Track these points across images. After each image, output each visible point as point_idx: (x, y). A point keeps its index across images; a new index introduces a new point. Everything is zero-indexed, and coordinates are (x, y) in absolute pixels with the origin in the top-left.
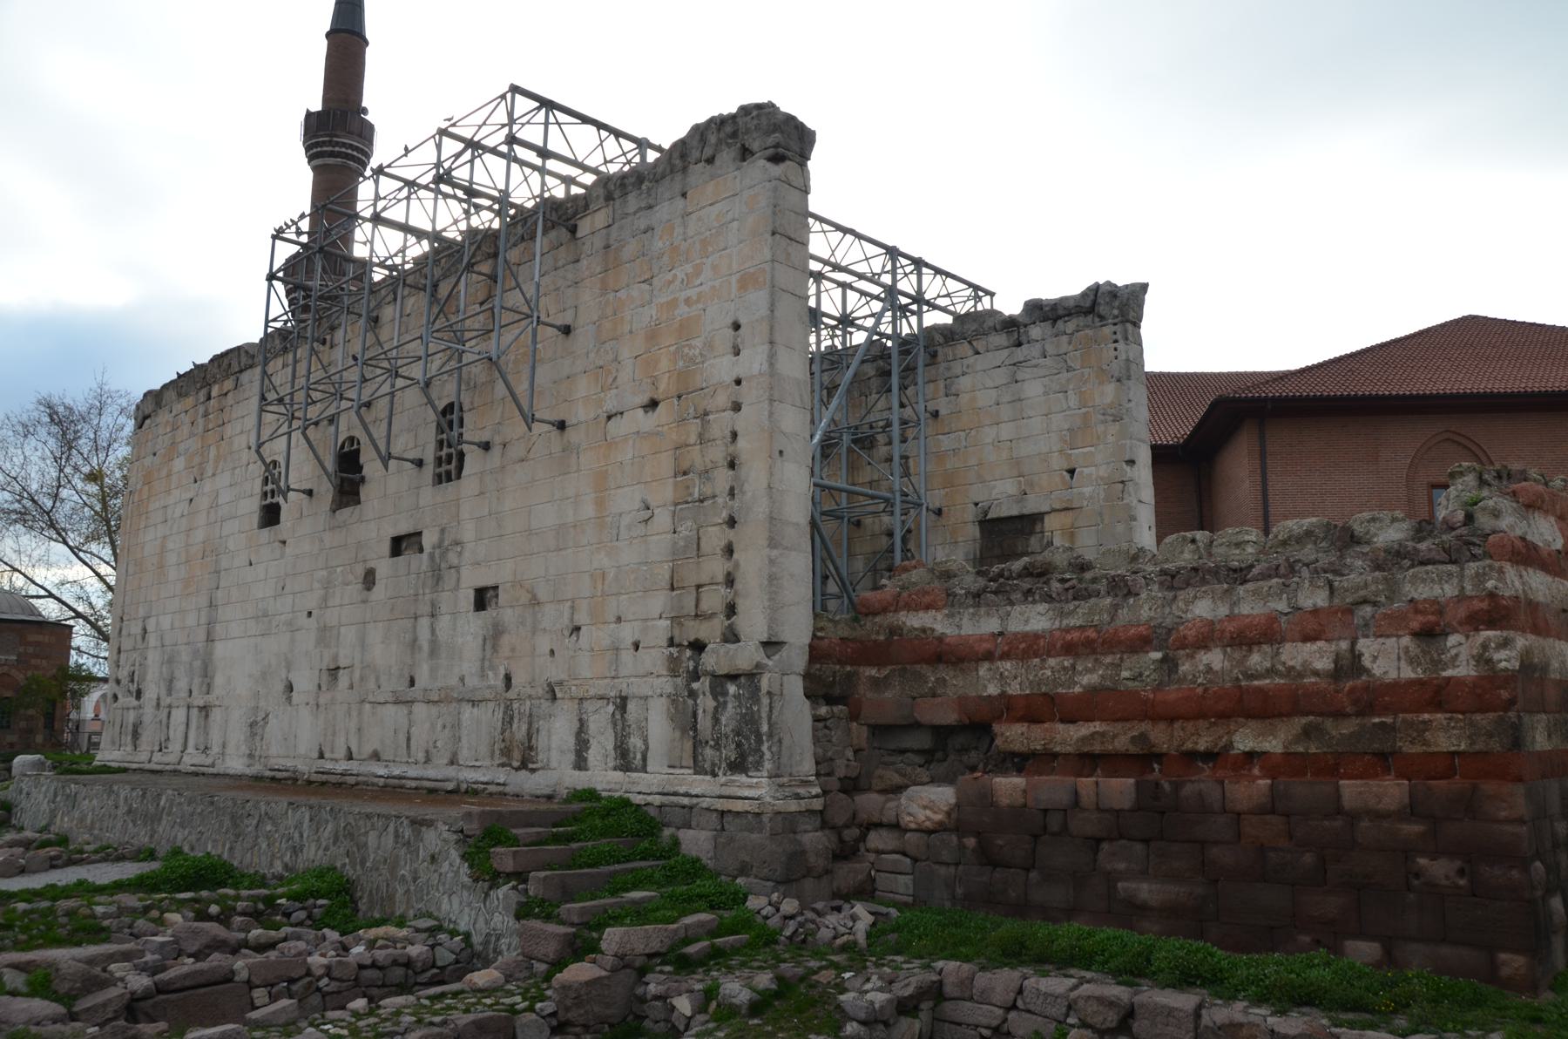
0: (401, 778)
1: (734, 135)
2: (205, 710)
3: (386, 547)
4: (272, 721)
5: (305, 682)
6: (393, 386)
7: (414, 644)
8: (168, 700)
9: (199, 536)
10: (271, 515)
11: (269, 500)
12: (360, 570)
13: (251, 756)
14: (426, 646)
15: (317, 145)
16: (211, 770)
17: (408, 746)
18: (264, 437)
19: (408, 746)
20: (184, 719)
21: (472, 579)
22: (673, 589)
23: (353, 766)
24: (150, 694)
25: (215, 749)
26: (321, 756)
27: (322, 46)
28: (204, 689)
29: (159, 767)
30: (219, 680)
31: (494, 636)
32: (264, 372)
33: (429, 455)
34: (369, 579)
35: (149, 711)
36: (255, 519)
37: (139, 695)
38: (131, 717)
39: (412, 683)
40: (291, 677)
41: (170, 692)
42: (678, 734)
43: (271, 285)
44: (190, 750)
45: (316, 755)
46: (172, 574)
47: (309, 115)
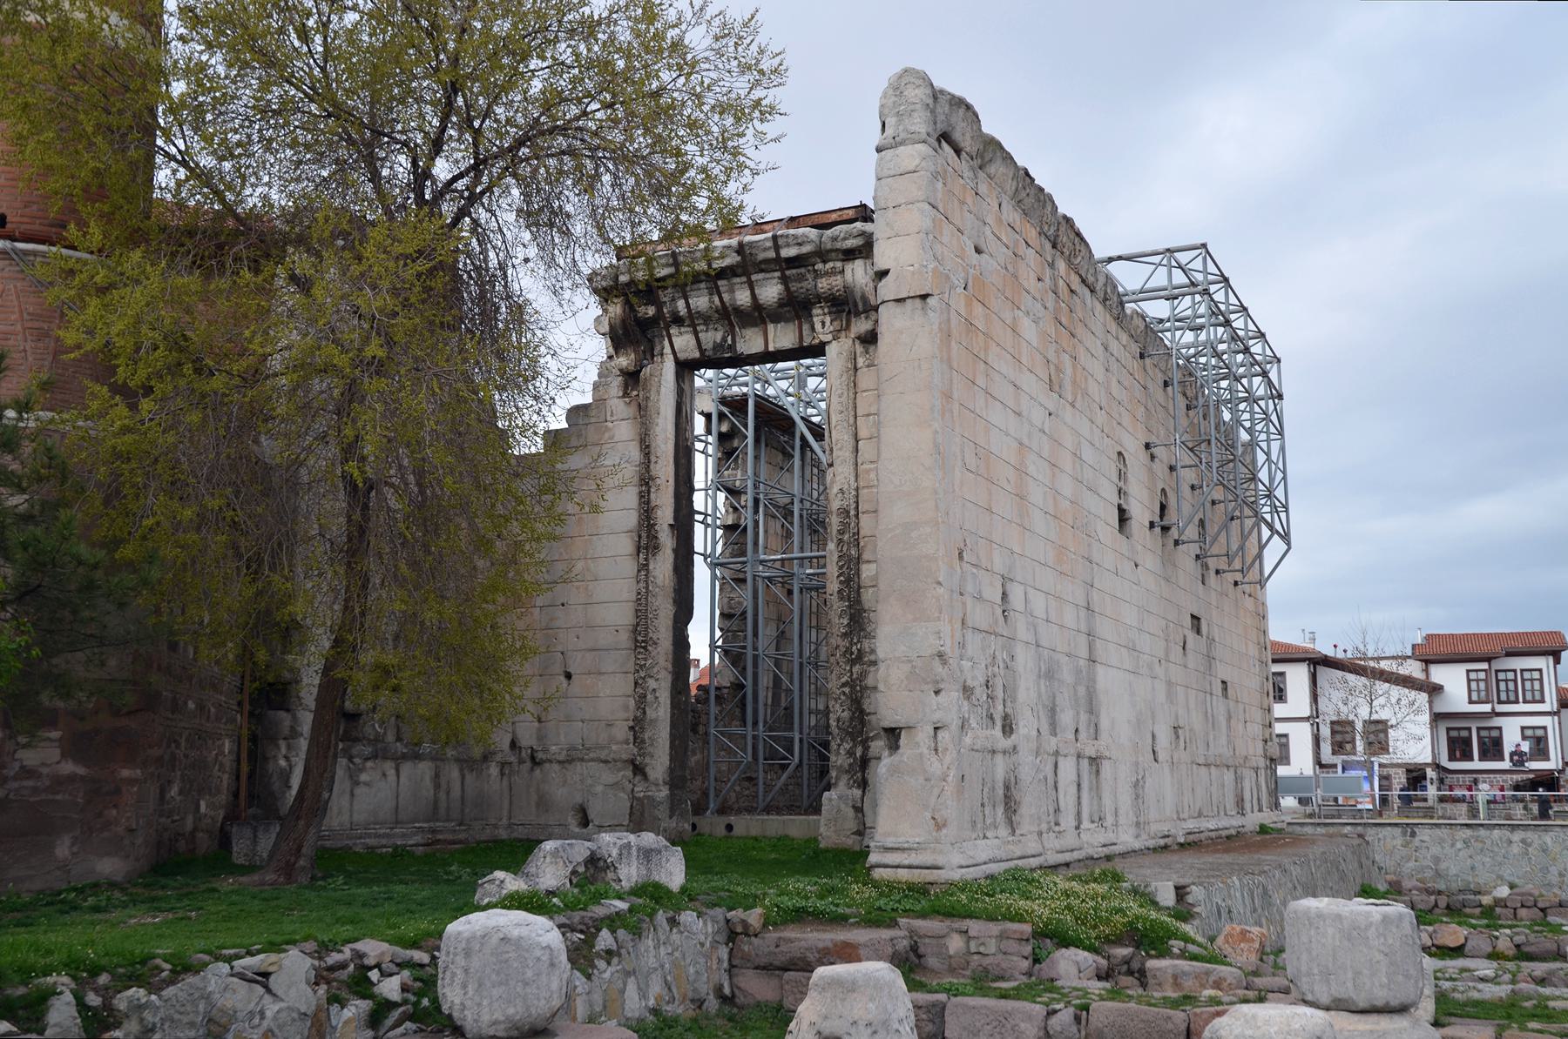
2: (1095, 761)
4: (1149, 781)
8: (1052, 743)
13: (1138, 824)
20: (1074, 777)
21: (1223, 672)
23: (1191, 825)
24: (1026, 725)
25: (1110, 820)
28: (1092, 730)
30: (1104, 723)
31: (1229, 718)
35: (1026, 758)
37: (1008, 729)
38: (1000, 767)
41: (1054, 729)
44: (1086, 824)
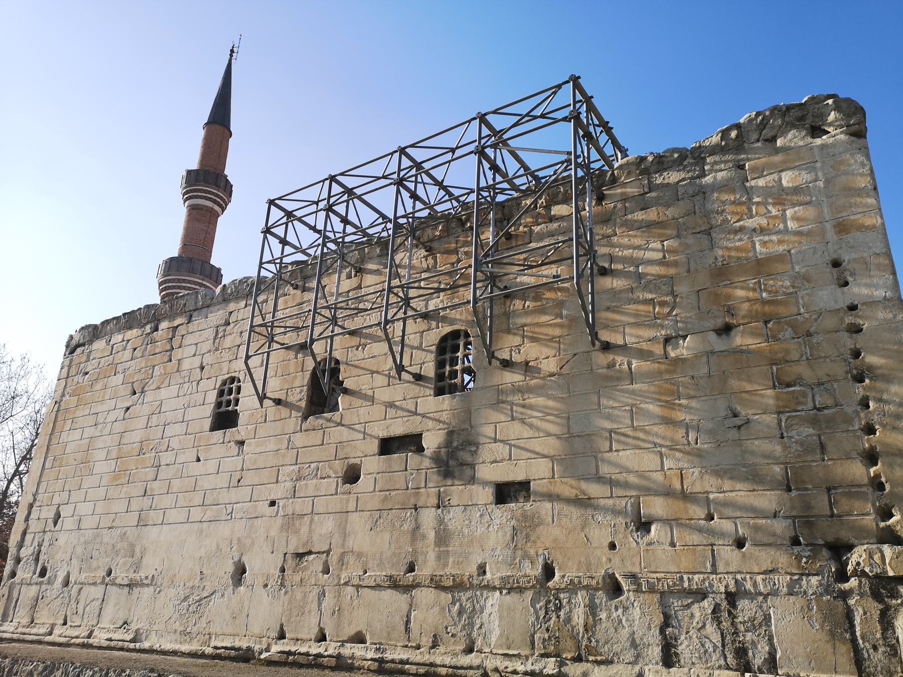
0: (402, 662)
1: (802, 119)
3: (375, 446)
5: (262, 564)
6: (405, 313)
7: (416, 532)
9: (136, 436)
10: (225, 419)
11: (223, 409)
12: (340, 467)
14: (431, 535)
15: (195, 191)
16: (132, 646)
17: (407, 630)
18: (250, 354)
19: (407, 630)
22: (789, 490)
26: (282, 636)
27: (201, 134)
29: (62, 640)
32: (256, 302)
33: (429, 370)
34: (352, 476)
36: (207, 423)
39: (411, 568)
40: (245, 559)
42: (823, 636)
43: (265, 238)
45: (274, 634)
46: (103, 467)
47: (189, 172)
